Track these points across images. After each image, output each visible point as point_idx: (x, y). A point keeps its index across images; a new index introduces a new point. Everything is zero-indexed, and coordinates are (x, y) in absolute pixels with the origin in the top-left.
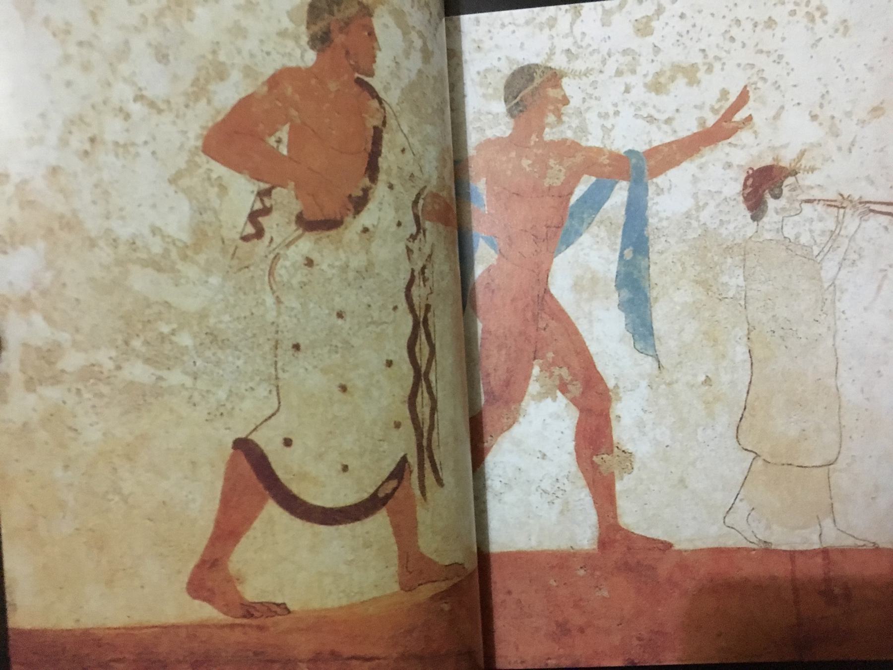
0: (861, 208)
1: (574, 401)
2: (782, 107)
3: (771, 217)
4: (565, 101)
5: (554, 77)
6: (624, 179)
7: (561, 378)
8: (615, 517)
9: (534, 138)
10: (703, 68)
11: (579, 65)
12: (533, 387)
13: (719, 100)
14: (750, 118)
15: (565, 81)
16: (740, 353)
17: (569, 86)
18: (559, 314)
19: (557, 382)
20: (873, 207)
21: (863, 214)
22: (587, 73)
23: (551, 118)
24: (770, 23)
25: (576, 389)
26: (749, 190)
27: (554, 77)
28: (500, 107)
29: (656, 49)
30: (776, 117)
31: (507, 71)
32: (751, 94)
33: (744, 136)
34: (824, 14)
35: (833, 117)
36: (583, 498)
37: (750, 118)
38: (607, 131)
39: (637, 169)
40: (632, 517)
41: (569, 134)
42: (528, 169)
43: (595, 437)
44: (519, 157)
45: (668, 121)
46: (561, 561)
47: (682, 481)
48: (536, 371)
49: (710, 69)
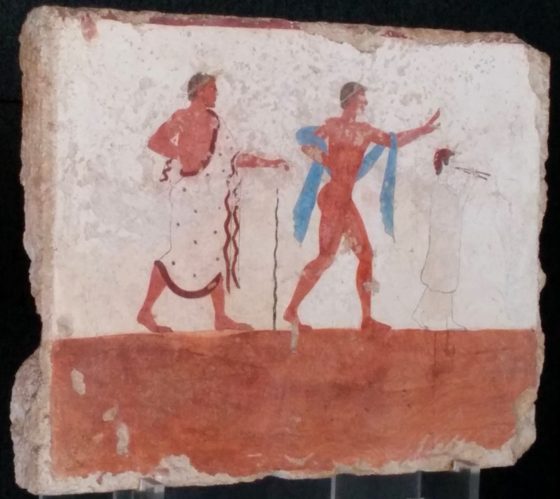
0: (476, 175)
1: (358, 255)
2: (452, 122)
3: (443, 174)
4: (366, 103)
5: (362, 90)
6: (387, 146)
7: (353, 243)
8: (369, 312)
9: (351, 120)
10: (424, 97)
11: (373, 86)
12: (341, 247)
13: (428, 114)
14: (439, 125)
15: (367, 93)
16: (426, 238)
17: (369, 96)
18: (355, 212)
19: (351, 245)
20: (481, 175)
21: (477, 177)
22: (375, 90)
23: (359, 111)
24: (451, 80)
25: (359, 249)
26: (436, 159)
27: (362, 90)
28: (337, 102)
29: (406, 84)
30: (449, 126)
31: (342, 83)
32: (441, 113)
33: (436, 133)
34: (471, 80)
35: (470, 130)
36: (357, 302)
37: (439, 125)
38: (383, 121)
39: (391, 141)
40: (377, 315)
41: (366, 120)
42: (348, 135)
43: (364, 274)
44: (344, 129)
45: (408, 120)
46: (345, 334)
47: (398, 297)
48: (343, 239)
49: (426, 98)
